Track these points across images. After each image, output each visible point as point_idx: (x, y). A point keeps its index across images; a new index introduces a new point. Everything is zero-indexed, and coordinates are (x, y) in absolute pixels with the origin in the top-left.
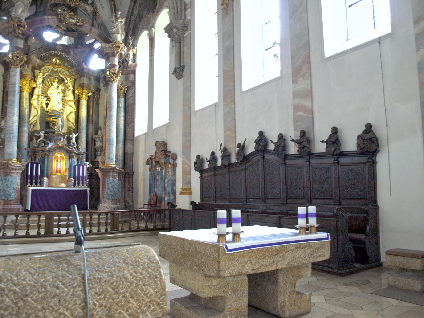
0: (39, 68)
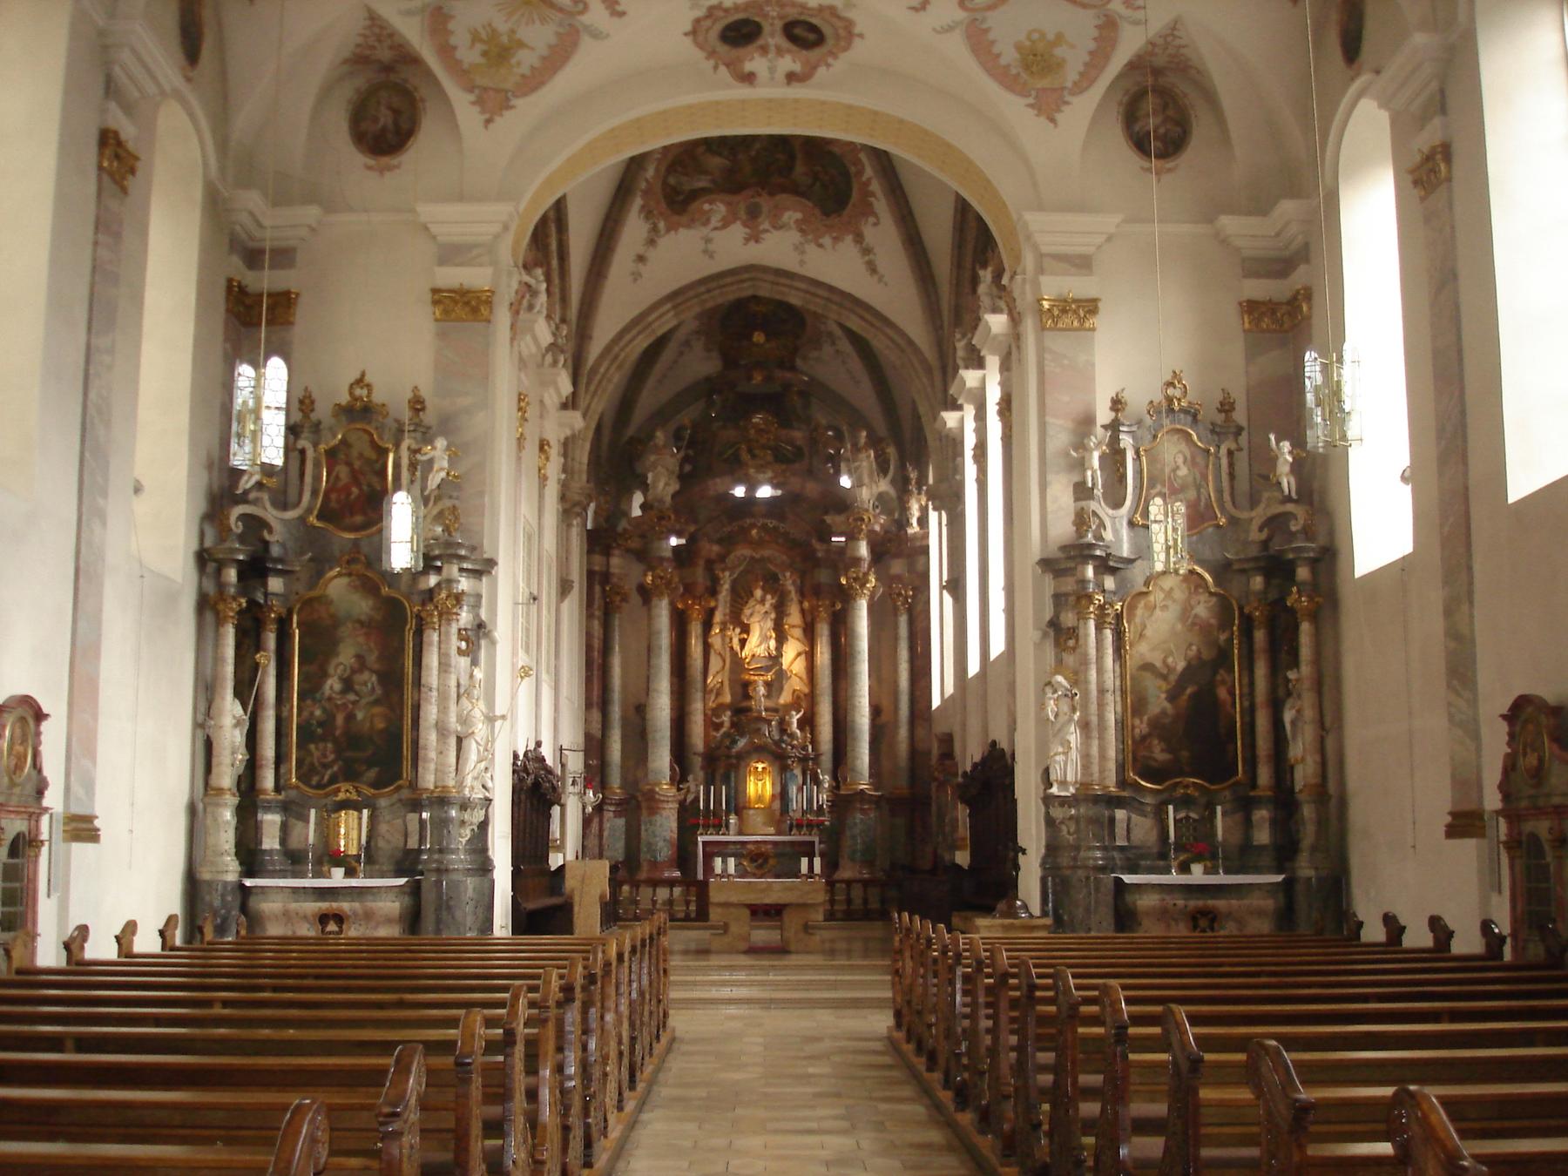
0: (722, 558)
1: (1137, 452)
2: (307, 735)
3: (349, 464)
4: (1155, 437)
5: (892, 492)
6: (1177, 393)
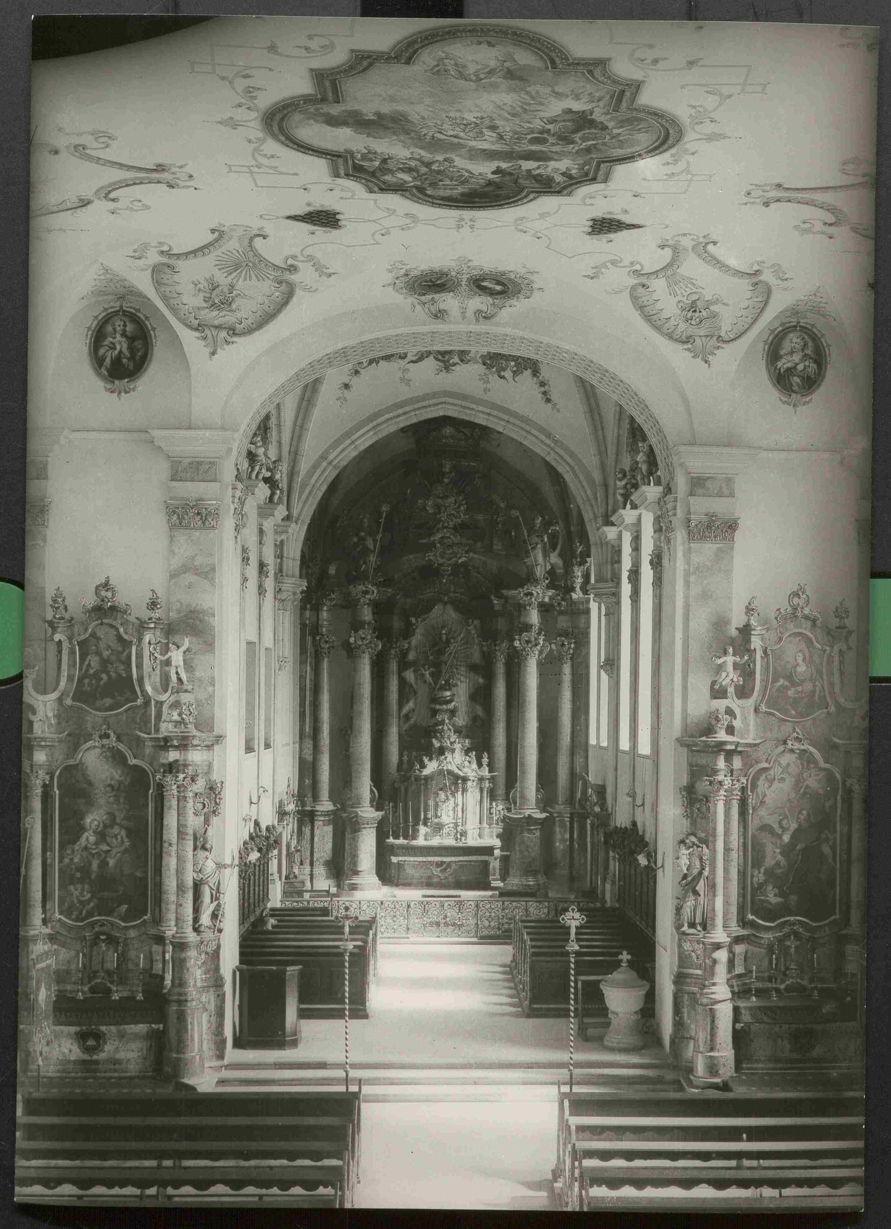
1: (765, 652)
2: (67, 879)
3: (98, 653)
4: (781, 639)
5: (560, 562)
6: (801, 602)
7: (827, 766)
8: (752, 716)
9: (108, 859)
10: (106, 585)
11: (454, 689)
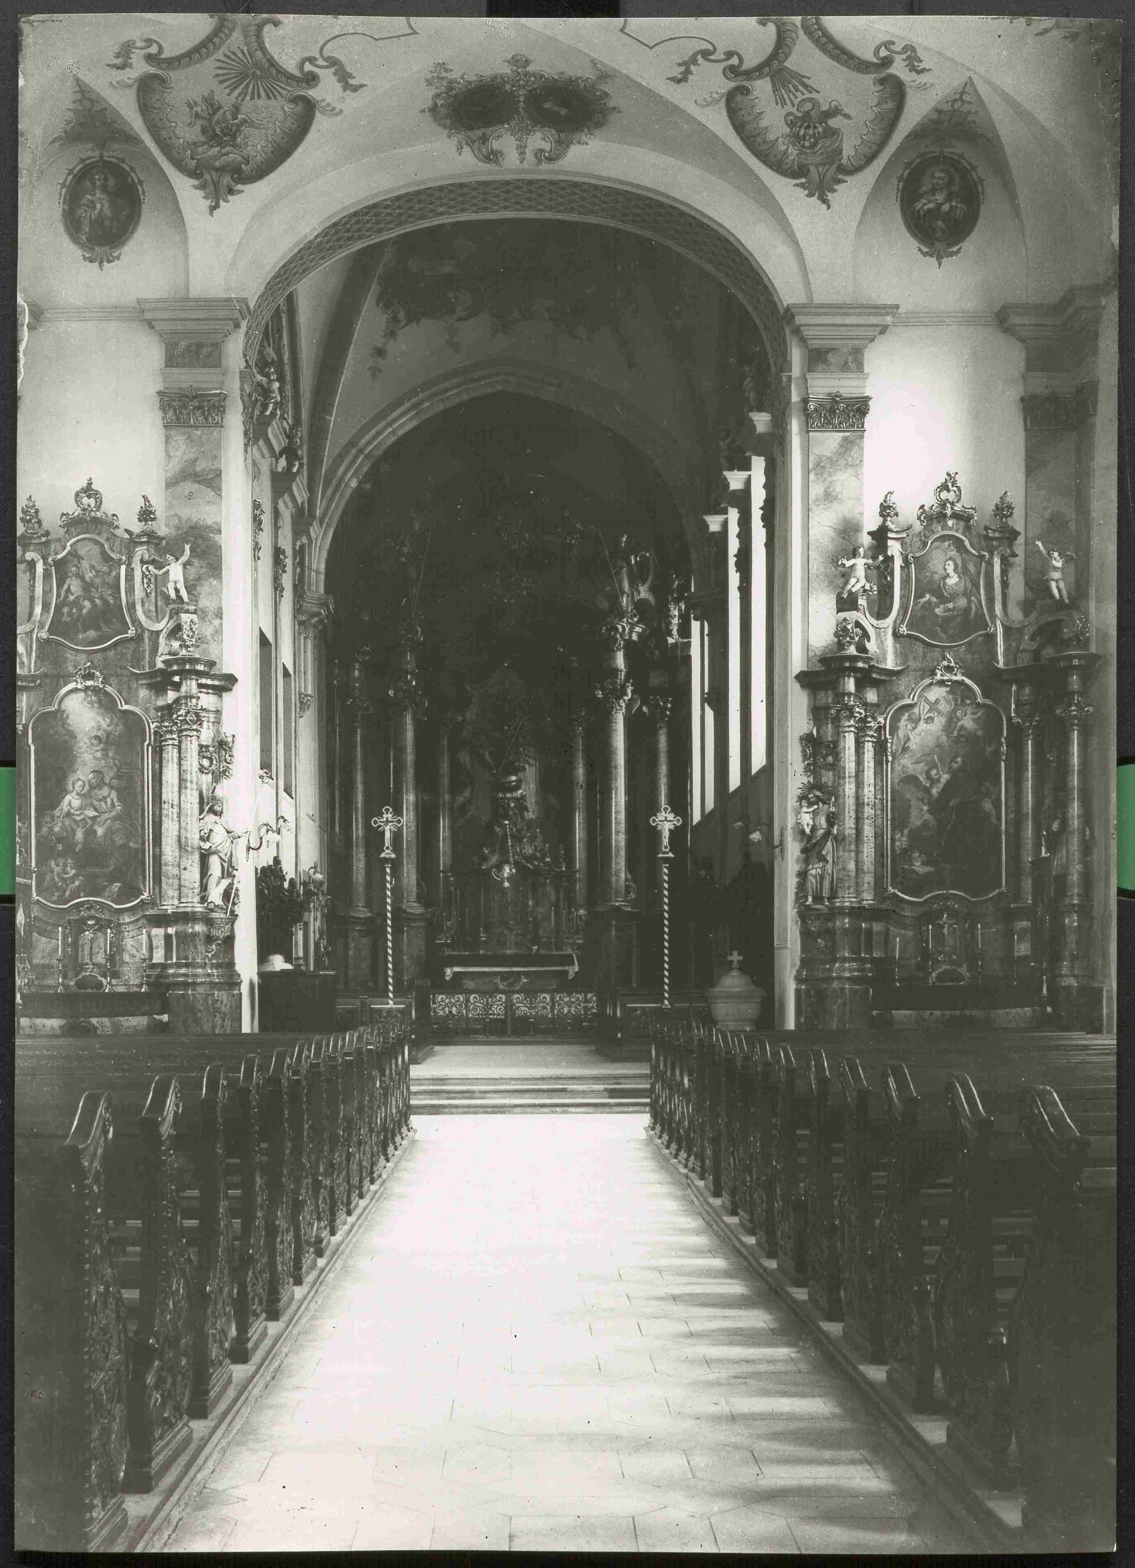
4: (925, 544)
5: (652, 599)
7: (987, 702)
8: (889, 640)
9: (96, 827)
10: (88, 490)
11: (521, 774)
